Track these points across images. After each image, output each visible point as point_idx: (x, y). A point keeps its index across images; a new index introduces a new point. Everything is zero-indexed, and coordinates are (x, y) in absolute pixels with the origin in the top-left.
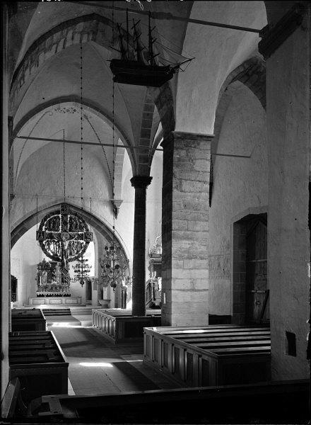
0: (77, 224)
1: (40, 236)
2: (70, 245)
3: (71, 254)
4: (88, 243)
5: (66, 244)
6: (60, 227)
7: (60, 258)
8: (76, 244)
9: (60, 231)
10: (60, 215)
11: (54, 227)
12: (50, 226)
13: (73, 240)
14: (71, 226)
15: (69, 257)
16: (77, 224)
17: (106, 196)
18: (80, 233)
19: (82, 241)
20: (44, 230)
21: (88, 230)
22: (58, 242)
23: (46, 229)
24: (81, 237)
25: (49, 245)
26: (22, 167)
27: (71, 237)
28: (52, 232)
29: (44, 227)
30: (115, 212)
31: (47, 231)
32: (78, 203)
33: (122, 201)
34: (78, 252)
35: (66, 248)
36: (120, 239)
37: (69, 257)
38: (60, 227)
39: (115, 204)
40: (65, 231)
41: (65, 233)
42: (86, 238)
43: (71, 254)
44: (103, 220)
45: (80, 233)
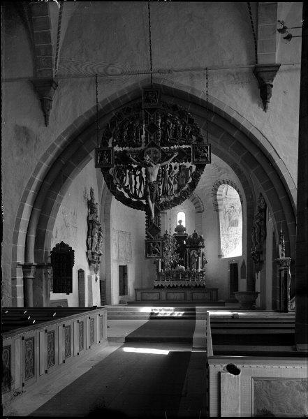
0: (177, 129)
1: (102, 159)
2: (162, 174)
3: (165, 193)
4: (201, 167)
5: (156, 170)
6: (143, 136)
7: (144, 202)
8: (177, 171)
9: (143, 147)
10: (143, 113)
11: (129, 137)
12: (121, 137)
13: (168, 163)
14: (164, 133)
15: (162, 200)
16: (177, 129)
17: (244, 60)
18: (184, 146)
19: (188, 165)
20: (110, 145)
21: (200, 140)
22: (139, 168)
23: (114, 144)
24: (183, 156)
25: (121, 176)
26: (71, 21)
27: (165, 157)
28: (127, 148)
29: (111, 140)
30: (263, 94)
31: (117, 149)
32: (182, 83)
33: (278, 66)
34: (180, 187)
35: (154, 179)
36: (274, 156)
37: (162, 200)
38: (143, 136)
39: (263, 75)
40: (153, 145)
41: (151, 149)
42: (197, 156)
43: (165, 193)
44: (234, 115)
45: (184, 146)
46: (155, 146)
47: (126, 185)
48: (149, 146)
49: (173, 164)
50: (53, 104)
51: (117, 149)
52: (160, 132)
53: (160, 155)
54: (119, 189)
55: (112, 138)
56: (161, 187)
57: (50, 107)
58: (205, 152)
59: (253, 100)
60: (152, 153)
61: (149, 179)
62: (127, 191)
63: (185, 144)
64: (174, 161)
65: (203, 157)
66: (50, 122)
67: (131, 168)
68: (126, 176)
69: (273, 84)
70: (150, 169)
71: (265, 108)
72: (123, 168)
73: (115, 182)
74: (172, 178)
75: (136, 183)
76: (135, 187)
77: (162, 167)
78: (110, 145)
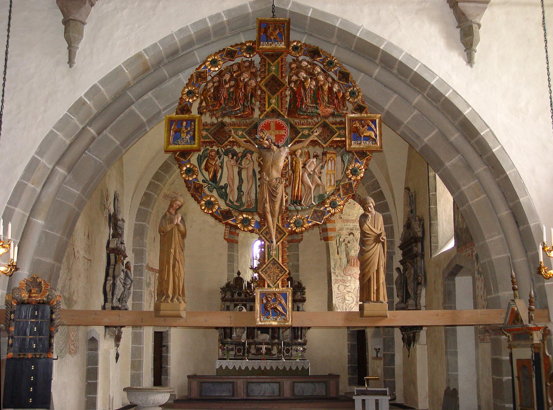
0: (319, 88)
16: (319, 88)
20: (194, 111)
28: (227, 120)
31: (207, 119)
40: (274, 113)
41: (272, 121)
46: (279, 115)
47: (222, 184)
48: (267, 116)
49: (311, 150)
50: (86, 29)
51: (207, 119)
52: (288, 93)
53: (286, 133)
54: (208, 192)
55: (199, 101)
56: (289, 190)
57: (81, 34)
58: (372, 130)
59: (450, 46)
60: (272, 125)
61: (268, 175)
62: (224, 196)
63: (333, 115)
64: (314, 143)
65: (368, 138)
66: (78, 59)
67: (234, 154)
68: (222, 167)
69: (481, 22)
70: (270, 157)
71: (470, 61)
72: (218, 152)
73: (201, 178)
74: (309, 175)
75: (241, 181)
76: (239, 189)
77: (293, 153)
78: (194, 111)
